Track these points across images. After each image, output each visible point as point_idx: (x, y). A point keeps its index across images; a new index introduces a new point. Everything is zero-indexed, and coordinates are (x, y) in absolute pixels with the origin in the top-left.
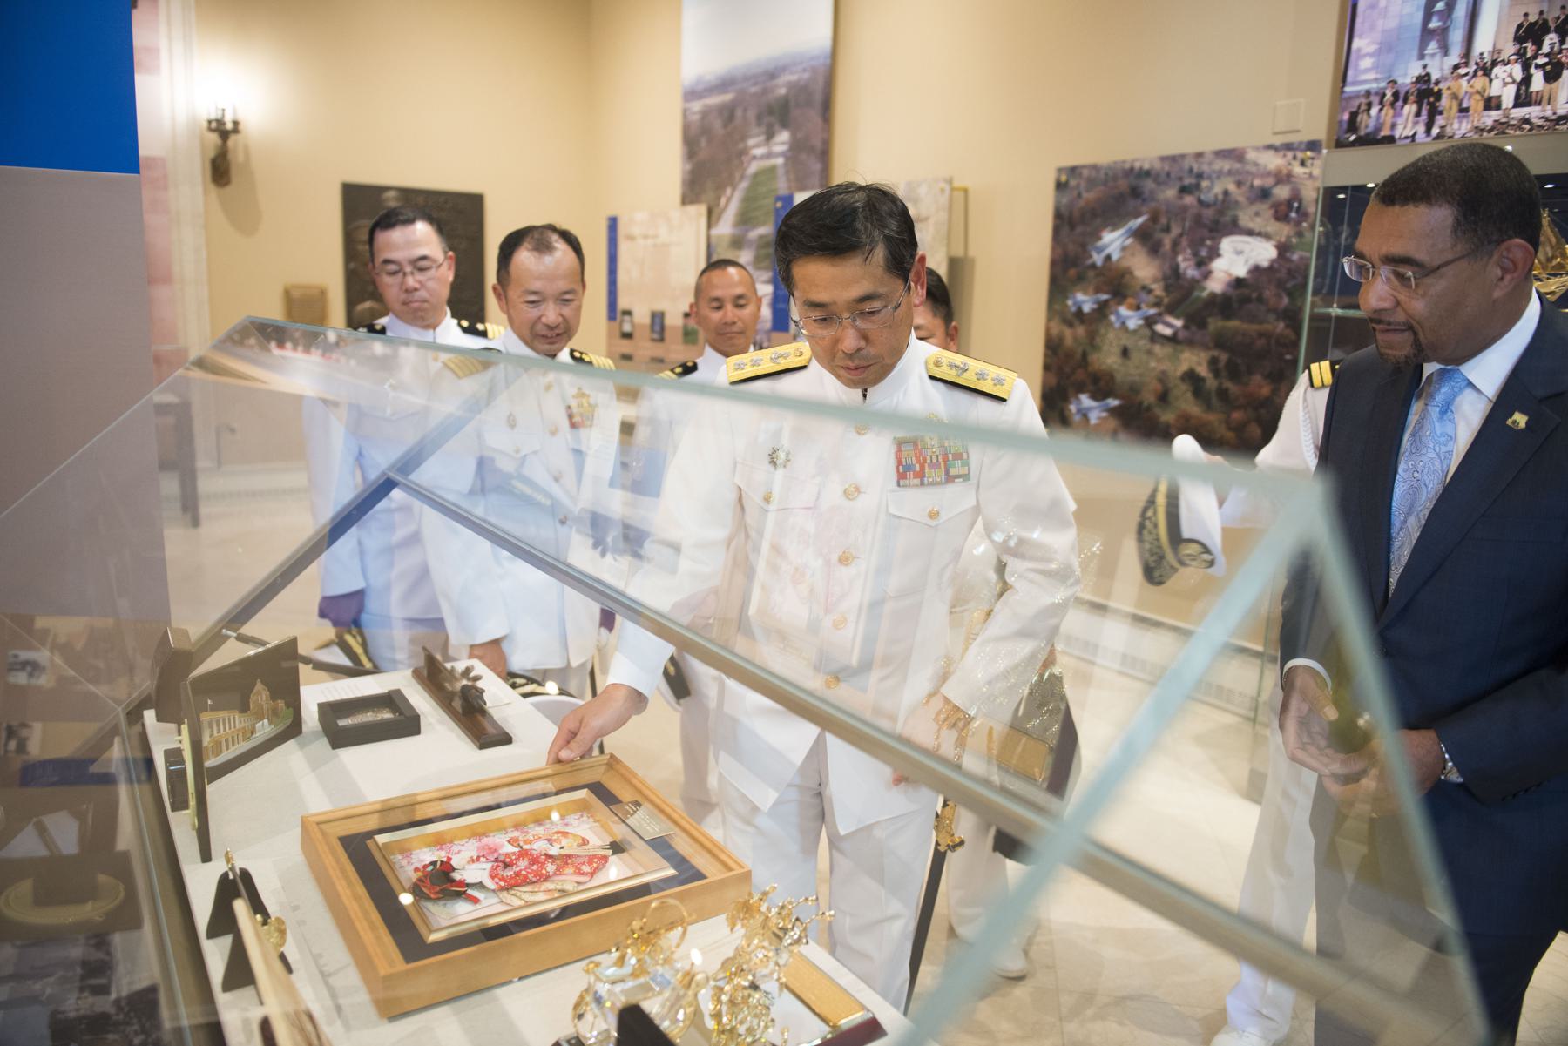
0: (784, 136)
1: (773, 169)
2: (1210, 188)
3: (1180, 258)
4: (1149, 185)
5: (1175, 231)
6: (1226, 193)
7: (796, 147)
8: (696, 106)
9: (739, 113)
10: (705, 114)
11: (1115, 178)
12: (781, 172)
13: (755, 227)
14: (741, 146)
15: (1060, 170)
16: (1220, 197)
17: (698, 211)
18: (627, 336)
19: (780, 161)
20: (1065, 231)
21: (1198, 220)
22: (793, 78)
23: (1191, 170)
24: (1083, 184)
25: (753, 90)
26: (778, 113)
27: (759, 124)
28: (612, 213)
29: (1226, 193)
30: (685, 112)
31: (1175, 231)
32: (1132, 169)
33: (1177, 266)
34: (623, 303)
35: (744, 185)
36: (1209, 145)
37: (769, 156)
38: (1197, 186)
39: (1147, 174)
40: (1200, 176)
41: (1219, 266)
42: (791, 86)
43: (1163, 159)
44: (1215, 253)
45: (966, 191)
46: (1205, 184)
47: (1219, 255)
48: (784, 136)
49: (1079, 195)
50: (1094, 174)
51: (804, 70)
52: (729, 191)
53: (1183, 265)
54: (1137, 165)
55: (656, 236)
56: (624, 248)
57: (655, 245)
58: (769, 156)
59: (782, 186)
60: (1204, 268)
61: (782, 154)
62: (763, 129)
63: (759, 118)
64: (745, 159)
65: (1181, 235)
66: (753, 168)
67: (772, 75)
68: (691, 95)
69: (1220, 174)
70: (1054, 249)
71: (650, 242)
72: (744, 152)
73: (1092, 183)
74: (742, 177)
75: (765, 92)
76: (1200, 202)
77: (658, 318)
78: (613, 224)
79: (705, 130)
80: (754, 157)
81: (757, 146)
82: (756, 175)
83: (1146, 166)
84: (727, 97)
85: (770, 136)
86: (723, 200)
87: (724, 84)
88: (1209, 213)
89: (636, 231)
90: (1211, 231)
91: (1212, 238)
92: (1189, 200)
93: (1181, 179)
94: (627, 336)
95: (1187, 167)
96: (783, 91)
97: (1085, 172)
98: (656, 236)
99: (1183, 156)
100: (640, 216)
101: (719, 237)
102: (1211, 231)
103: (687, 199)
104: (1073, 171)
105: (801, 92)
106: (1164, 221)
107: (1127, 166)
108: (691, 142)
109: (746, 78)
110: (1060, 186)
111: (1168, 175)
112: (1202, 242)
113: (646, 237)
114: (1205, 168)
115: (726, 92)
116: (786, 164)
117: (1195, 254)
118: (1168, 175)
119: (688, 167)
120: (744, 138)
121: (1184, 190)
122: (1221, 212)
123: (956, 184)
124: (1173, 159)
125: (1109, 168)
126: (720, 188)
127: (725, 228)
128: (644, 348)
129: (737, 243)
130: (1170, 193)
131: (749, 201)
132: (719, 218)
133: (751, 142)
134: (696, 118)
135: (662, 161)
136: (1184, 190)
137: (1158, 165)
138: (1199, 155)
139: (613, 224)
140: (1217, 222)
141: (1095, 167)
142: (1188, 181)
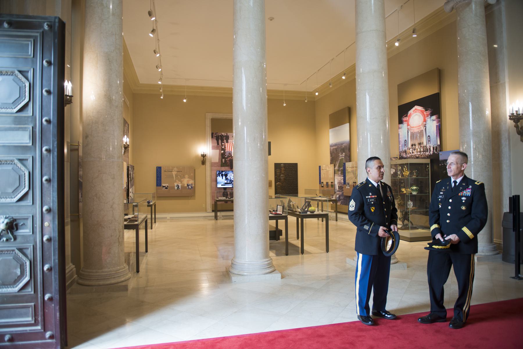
7: (345, 155)
8: (332, 148)
10: (333, 149)
17: (333, 165)
18: (323, 187)
26: (343, 150)
34: (322, 181)
56: (322, 171)
59: (344, 161)
67: (342, 144)
68: (331, 146)
77: (327, 183)
78: (320, 167)
79: (333, 152)
87: (336, 145)
94: (323, 187)
100: (324, 166)
105: (346, 147)
108: (331, 154)
126: (336, 161)
127: (337, 168)
128: (325, 188)
129: (338, 170)
135: (326, 157)
139: (320, 167)
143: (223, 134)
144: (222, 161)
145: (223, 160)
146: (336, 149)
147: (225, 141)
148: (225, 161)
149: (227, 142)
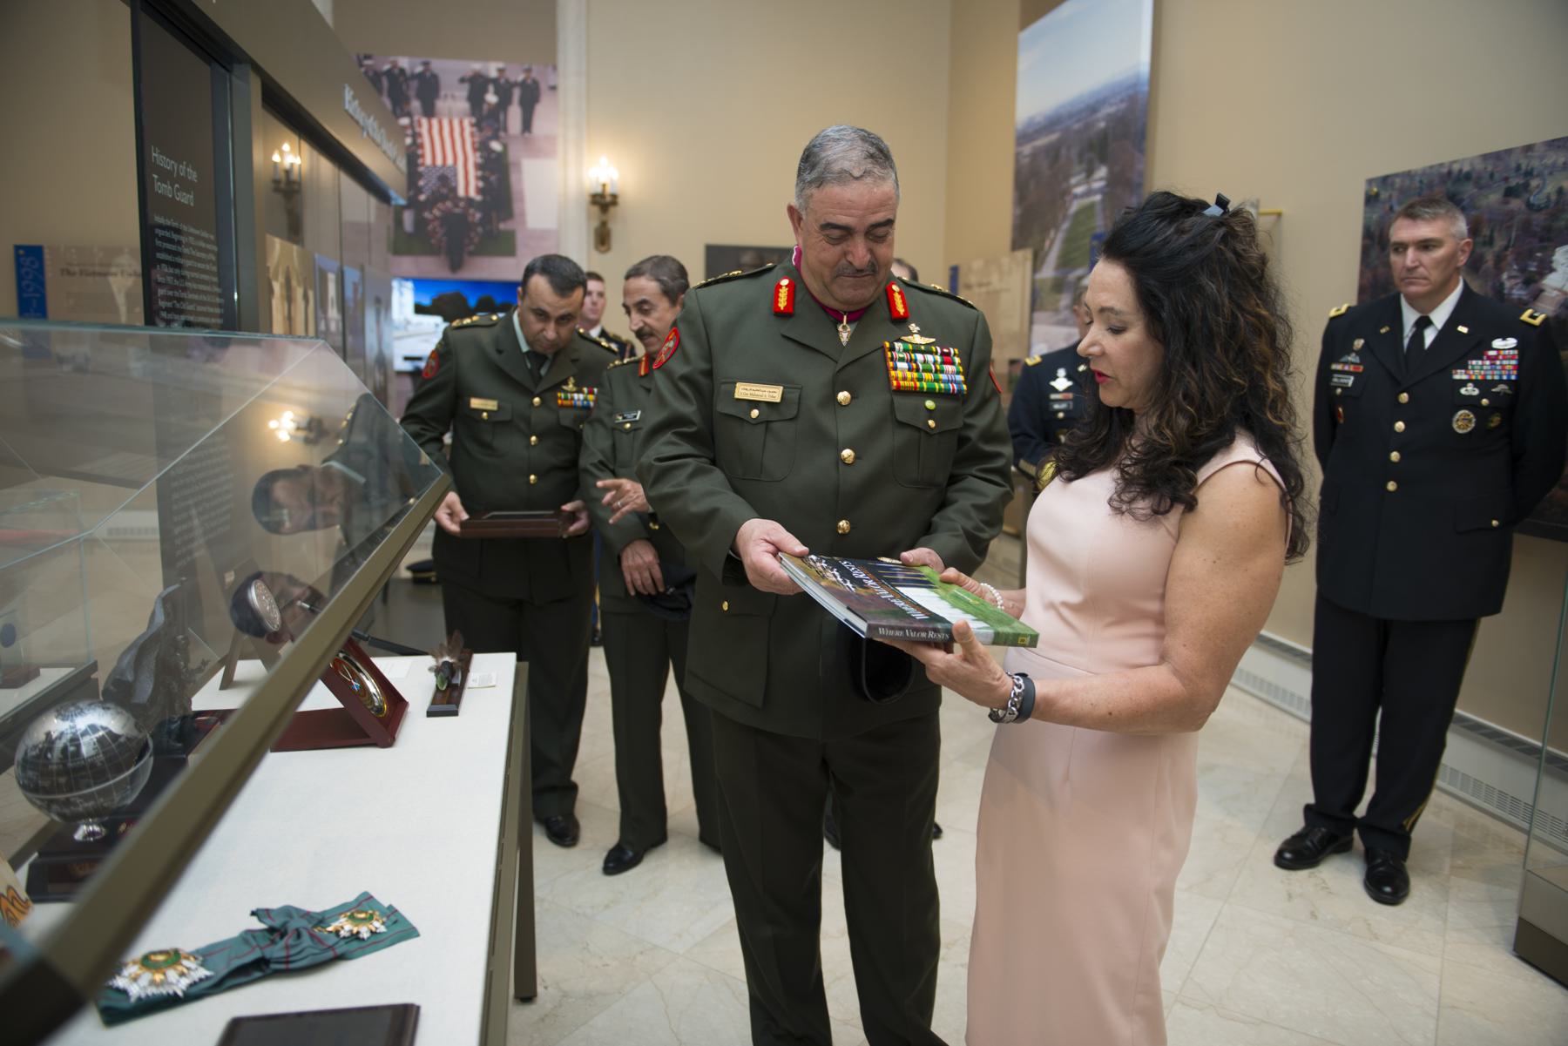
0: (1102, 172)
1: (1092, 206)
2: (1540, 188)
3: (1505, 276)
4: (1469, 190)
5: (1499, 243)
6: (1560, 191)
7: (1113, 181)
8: (1027, 149)
9: (1063, 151)
10: (1034, 155)
11: (1431, 185)
12: (1098, 209)
13: (1074, 268)
14: (1064, 185)
15: (1370, 182)
16: (1553, 197)
17: (1026, 255)
19: (1098, 198)
20: (1375, 252)
21: (1526, 227)
22: (1108, 110)
23: (1518, 168)
24: (1395, 194)
25: (1076, 126)
27: (1081, 162)
28: (954, 263)
29: (1560, 191)
30: (1018, 155)
31: (1499, 243)
32: (1450, 173)
33: (1502, 284)
35: (1066, 226)
36: (1539, 136)
37: (1089, 193)
38: (1526, 186)
39: (1467, 177)
40: (1529, 174)
41: (1552, 281)
42: (1110, 118)
43: (1485, 157)
44: (1547, 268)
45: (1279, 215)
46: (1534, 183)
47: (1552, 270)
48: (1102, 172)
49: (1391, 208)
50: (1407, 182)
51: (1122, 101)
52: (1052, 233)
53: (1507, 284)
54: (1456, 167)
55: (988, 284)
57: (988, 293)
58: (1089, 193)
60: (1533, 287)
61: (1100, 191)
62: (1084, 166)
63: (1081, 155)
64: (1068, 198)
65: (1506, 248)
66: (1075, 206)
67: (1093, 109)
68: (1023, 137)
69: (1553, 169)
70: (1362, 274)
71: (984, 289)
72: (1067, 192)
73: (1403, 192)
74: (1065, 218)
75: (1087, 126)
76: (1529, 205)
80: (1076, 197)
81: (1078, 184)
82: (1077, 214)
83: (1466, 168)
84: (1054, 137)
85: (1090, 172)
86: (1047, 243)
87: (1052, 123)
88: (1539, 219)
89: (973, 279)
90: (1542, 240)
91: (1542, 249)
92: (1516, 204)
93: (1506, 179)
95: (1513, 165)
96: (1102, 125)
97: (1398, 180)
98: (988, 284)
99: (1509, 152)
100: (977, 264)
101: (1043, 281)
102: (1542, 240)
103: (1016, 245)
104: (1385, 180)
106: (1486, 232)
107: (1445, 170)
109: (1070, 116)
110: (1371, 200)
111: (1492, 176)
112: (1530, 254)
113: (981, 285)
114: (1535, 163)
115: (1053, 132)
116: (1103, 201)
117: (1523, 270)
118: (1492, 176)
119: (1018, 212)
120: (1067, 177)
121: (1510, 193)
122: (1554, 216)
123: (1262, 210)
124: (1497, 156)
125: (1424, 173)
127: (1048, 272)
130: (1493, 198)
131: (1068, 241)
132: (1043, 262)
133: (1073, 181)
134: (1026, 161)
135: (998, 206)
136: (1510, 193)
137: (1479, 166)
138: (1528, 148)
140: (1548, 229)
141: (1408, 175)
142: (1513, 182)
143: (403, 62)
144: (399, 222)
145: (408, 218)
146: (1053, 152)
147: (416, 105)
148: (420, 223)
149: (429, 112)
